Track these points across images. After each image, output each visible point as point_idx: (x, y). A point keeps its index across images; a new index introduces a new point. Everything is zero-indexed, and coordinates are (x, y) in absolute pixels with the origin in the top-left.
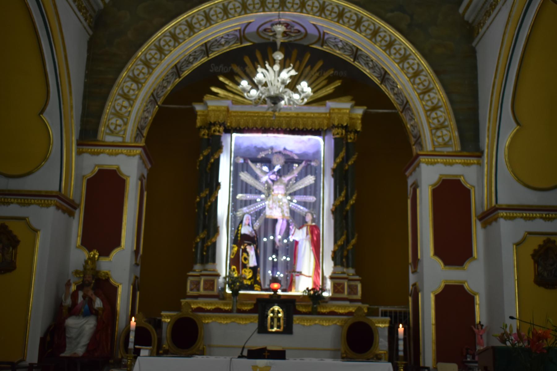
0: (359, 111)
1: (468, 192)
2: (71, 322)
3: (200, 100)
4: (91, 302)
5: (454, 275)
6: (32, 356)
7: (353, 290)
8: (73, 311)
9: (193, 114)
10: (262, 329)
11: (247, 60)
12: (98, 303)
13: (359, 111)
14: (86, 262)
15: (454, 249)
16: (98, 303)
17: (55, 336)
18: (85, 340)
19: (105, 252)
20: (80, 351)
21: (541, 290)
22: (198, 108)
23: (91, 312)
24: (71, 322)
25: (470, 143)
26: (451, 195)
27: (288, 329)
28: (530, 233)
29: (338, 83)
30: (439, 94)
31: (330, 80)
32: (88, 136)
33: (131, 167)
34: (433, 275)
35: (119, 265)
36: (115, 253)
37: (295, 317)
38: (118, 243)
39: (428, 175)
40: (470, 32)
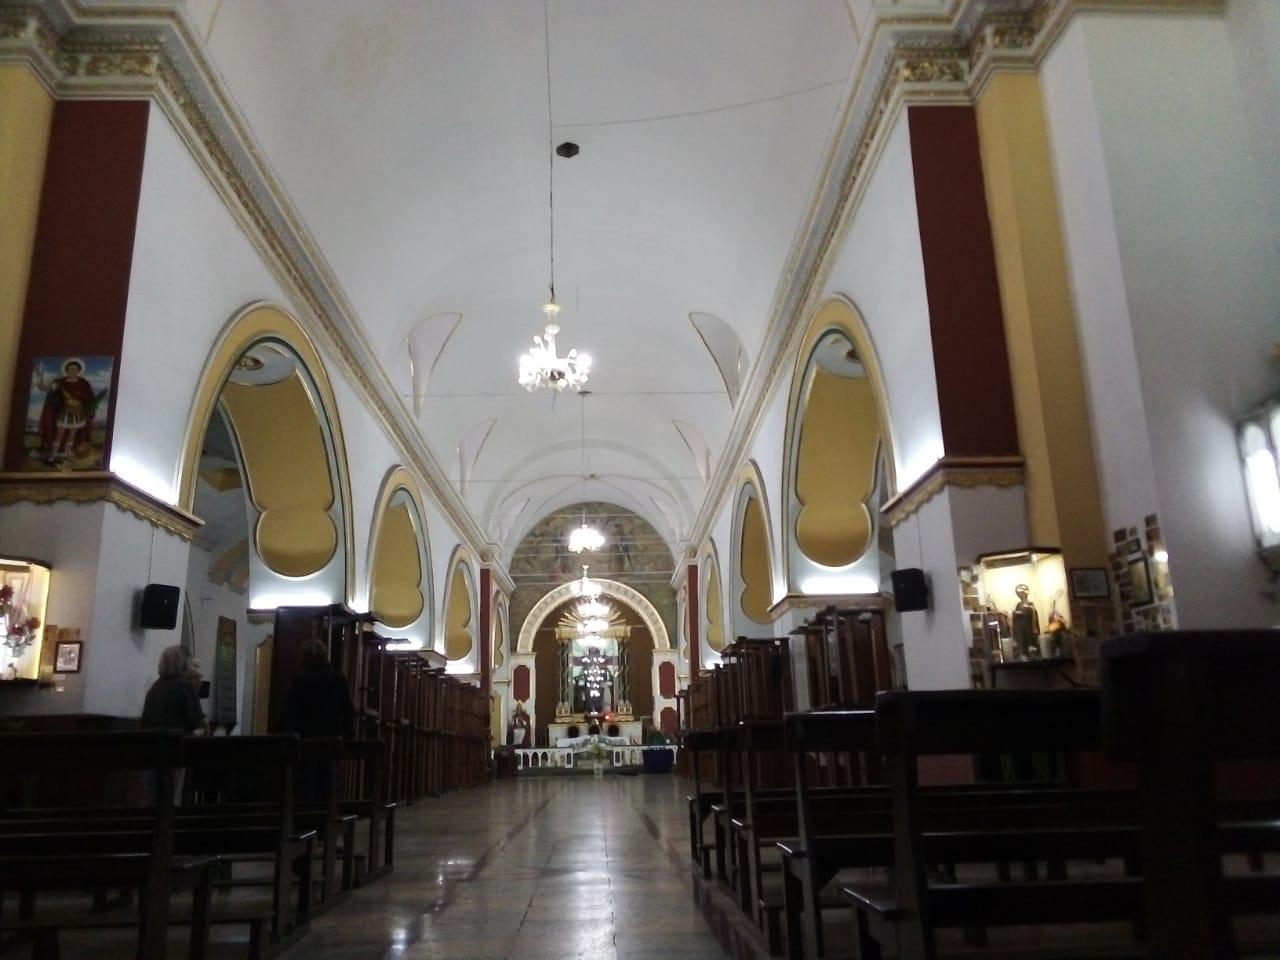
0: (629, 628)
1: (673, 667)
2: (516, 731)
3: (557, 626)
4: (522, 723)
6: (504, 742)
7: (628, 710)
8: (515, 726)
9: (554, 633)
12: (525, 723)
13: (629, 628)
14: (519, 707)
16: (525, 723)
17: (510, 736)
19: (524, 701)
22: (557, 630)
23: (522, 726)
24: (516, 731)
25: (674, 643)
29: (618, 614)
31: (615, 612)
32: (513, 649)
33: (530, 663)
35: (530, 706)
36: (528, 701)
38: (528, 696)
39: (658, 660)
40: (674, 593)
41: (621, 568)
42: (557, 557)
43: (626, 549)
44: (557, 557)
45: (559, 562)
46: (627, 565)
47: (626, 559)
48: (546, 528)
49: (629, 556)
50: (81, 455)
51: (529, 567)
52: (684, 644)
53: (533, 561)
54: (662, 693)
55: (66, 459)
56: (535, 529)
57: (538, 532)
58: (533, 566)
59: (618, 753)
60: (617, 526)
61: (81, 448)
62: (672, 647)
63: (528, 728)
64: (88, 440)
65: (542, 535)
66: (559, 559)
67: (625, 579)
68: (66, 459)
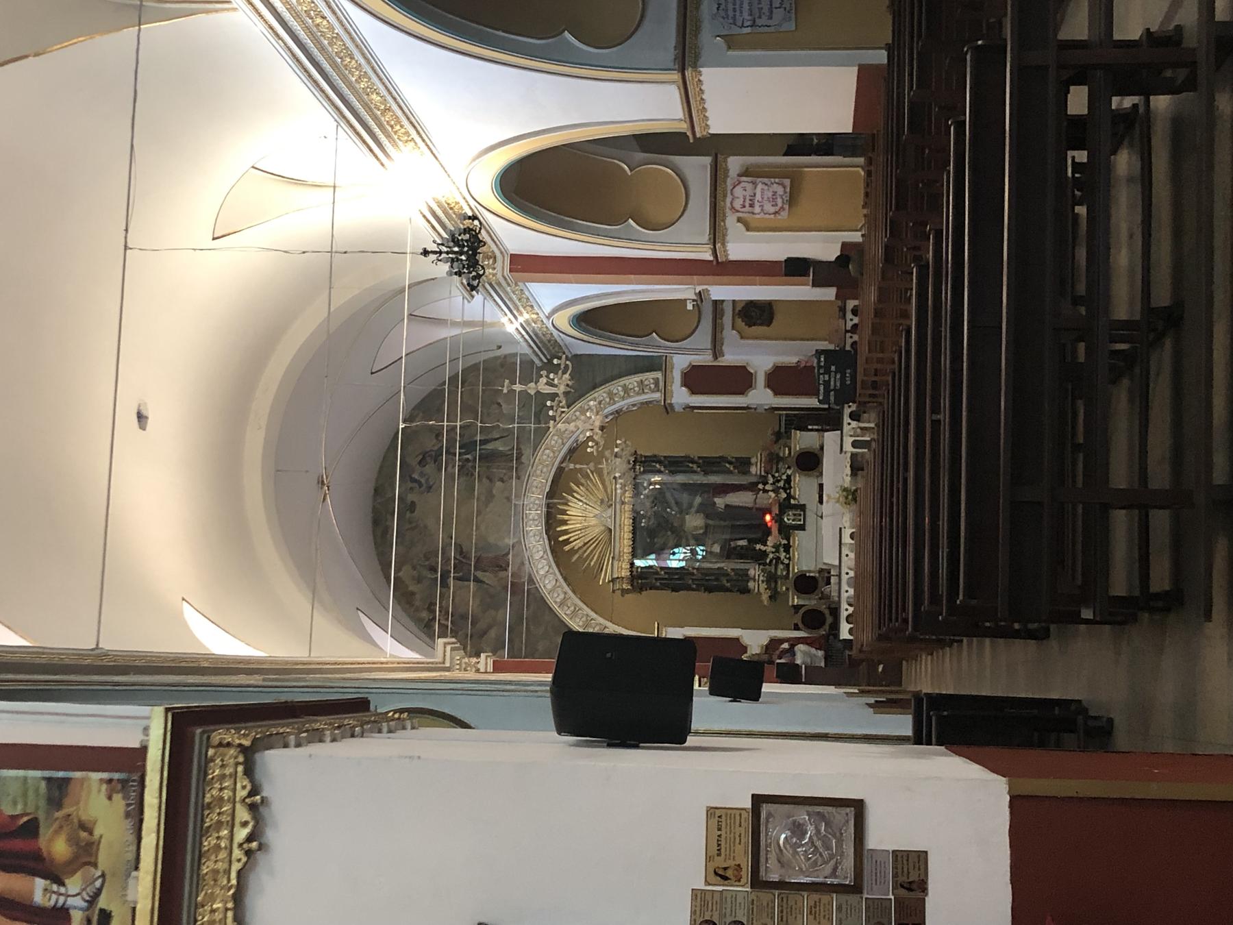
4: (785, 651)
5: (761, 380)
10: (802, 528)
11: (567, 548)
12: (786, 646)
15: (739, 379)
18: (813, 650)
20: (820, 653)
21: (775, 323)
23: (791, 651)
26: (697, 379)
27: (803, 508)
28: (733, 328)
30: (616, 387)
34: (760, 396)
37: (792, 502)
38: (736, 640)
41: (507, 457)
42: (477, 580)
43: (468, 446)
44: (477, 580)
45: (486, 577)
46: (500, 446)
47: (490, 446)
48: (418, 596)
49: (483, 442)
50: (85, 853)
51: (493, 633)
52: (652, 347)
53: (481, 625)
54: (742, 392)
55: (92, 901)
56: (418, 621)
57: (425, 615)
58: (490, 627)
59: (854, 444)
60: (422, 463)
61: (59, 848)
62: (660, 370)
63: (794, 642)
64: (31, 829)
65: (431, 608)
66: (479, 574)
67: (527, 451)
68: (92, 901)
